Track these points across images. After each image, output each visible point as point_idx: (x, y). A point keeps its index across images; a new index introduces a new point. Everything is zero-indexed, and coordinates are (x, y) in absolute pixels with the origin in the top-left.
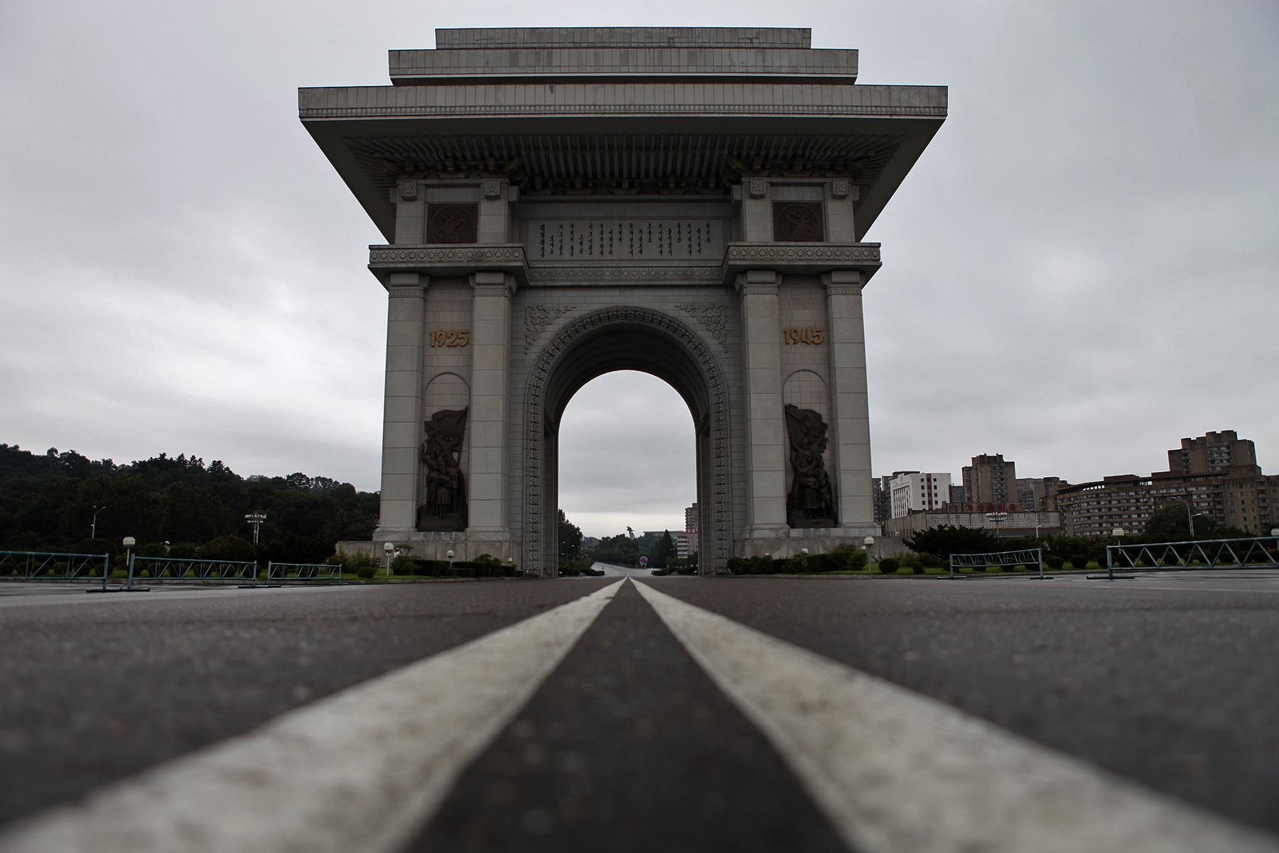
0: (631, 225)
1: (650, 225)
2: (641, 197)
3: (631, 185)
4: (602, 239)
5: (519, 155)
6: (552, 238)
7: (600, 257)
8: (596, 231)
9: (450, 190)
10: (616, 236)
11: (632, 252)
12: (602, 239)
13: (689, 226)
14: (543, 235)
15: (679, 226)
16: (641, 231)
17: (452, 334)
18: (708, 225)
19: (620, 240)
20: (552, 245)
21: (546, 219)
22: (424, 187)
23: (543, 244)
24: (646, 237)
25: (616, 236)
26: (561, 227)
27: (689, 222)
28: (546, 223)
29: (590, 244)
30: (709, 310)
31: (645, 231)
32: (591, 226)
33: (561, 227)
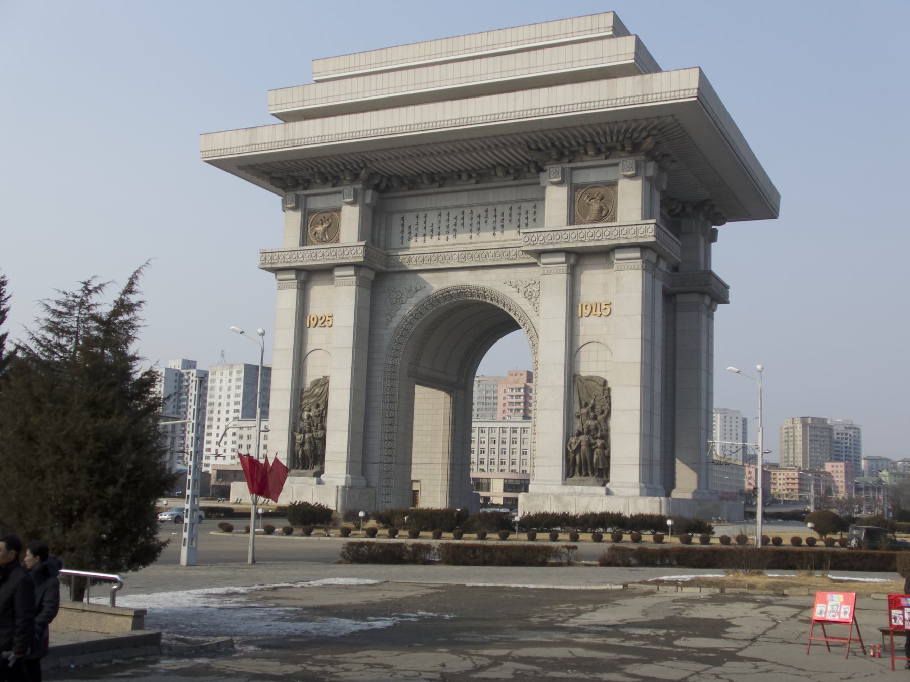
2: (479, 186)
3: (470, 177)
4: (448, 227)
5: (365, 165)
6: (410, 227)
7: (446, 243)
8: (444, 217)
9: (323, 197)
10: (459, 222)
14: (403, 225)
15: (510, 209)
16: (479, 216)
17: (322, 317)
18: (535, 207)
19: (463, 224)
20: (410, 233)
21: (406, 211)
22: (304, 197)
23: (403, 234)
24: (483, 220)
25: (459, 222)
28: (407, 216)
30: (531, 286)
31: (483, 215)
32: (440, 215)
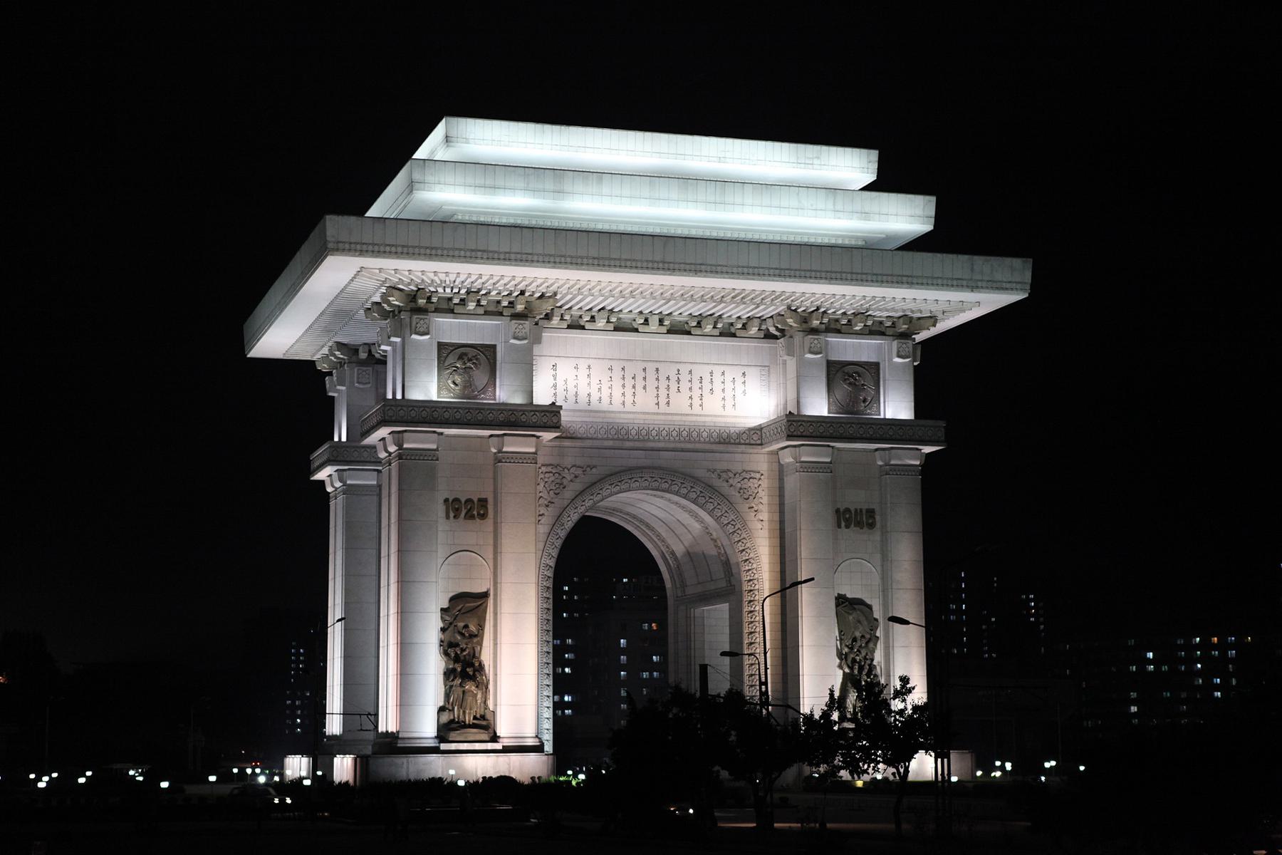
0: (657, 370)
1: (679, 371)
4: (624, 386)
10: (640, 384)
11: (658, 404)
12: (624, 386)
13: (723, 373)
15: (711, 373)
19: (645, 388)
25: (640, 384)
26: (576, 368)
27: (722, 368)
29: (610, 391)
31: (674, 378)
33: (576, 368)
